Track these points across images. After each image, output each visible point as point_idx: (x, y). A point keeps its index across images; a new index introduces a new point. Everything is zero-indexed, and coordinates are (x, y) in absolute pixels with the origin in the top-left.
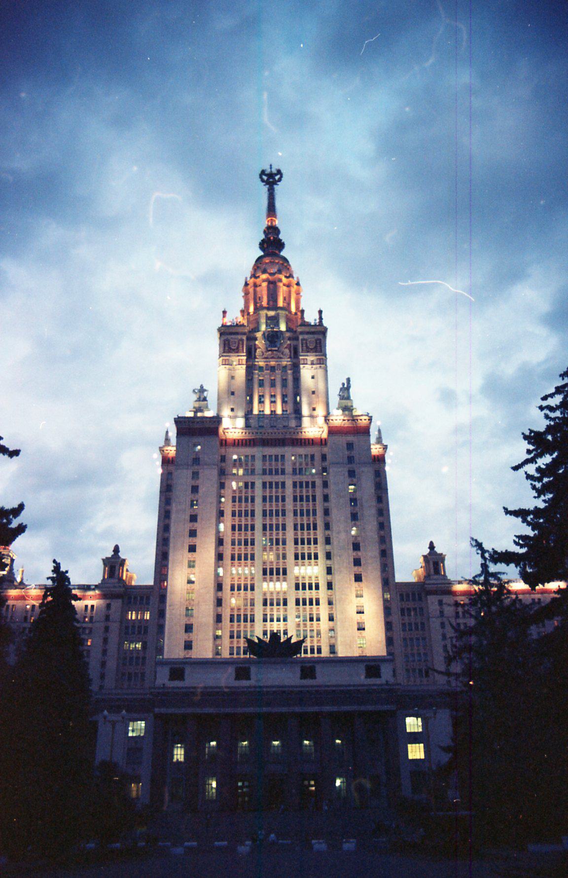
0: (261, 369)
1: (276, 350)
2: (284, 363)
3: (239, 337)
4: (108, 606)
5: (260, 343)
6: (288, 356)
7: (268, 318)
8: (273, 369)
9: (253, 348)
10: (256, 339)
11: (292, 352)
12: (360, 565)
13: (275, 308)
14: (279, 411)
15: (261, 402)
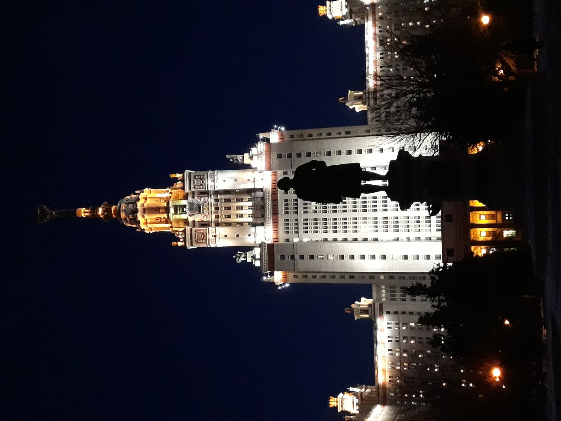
0: (217, 217)
1: (203, 207)
2: (213, 201)
3: (194, 233)
4: (388, 313)
5: (198, 218)
6: (207, 198)
7: (176, 213)
8: (217, 209)
9: (200, 223)
10: (194, 221)
11: (202, 195)
12: (361, 150)
13: (167, 210)
14: (250, 204)
15: (241, 216)
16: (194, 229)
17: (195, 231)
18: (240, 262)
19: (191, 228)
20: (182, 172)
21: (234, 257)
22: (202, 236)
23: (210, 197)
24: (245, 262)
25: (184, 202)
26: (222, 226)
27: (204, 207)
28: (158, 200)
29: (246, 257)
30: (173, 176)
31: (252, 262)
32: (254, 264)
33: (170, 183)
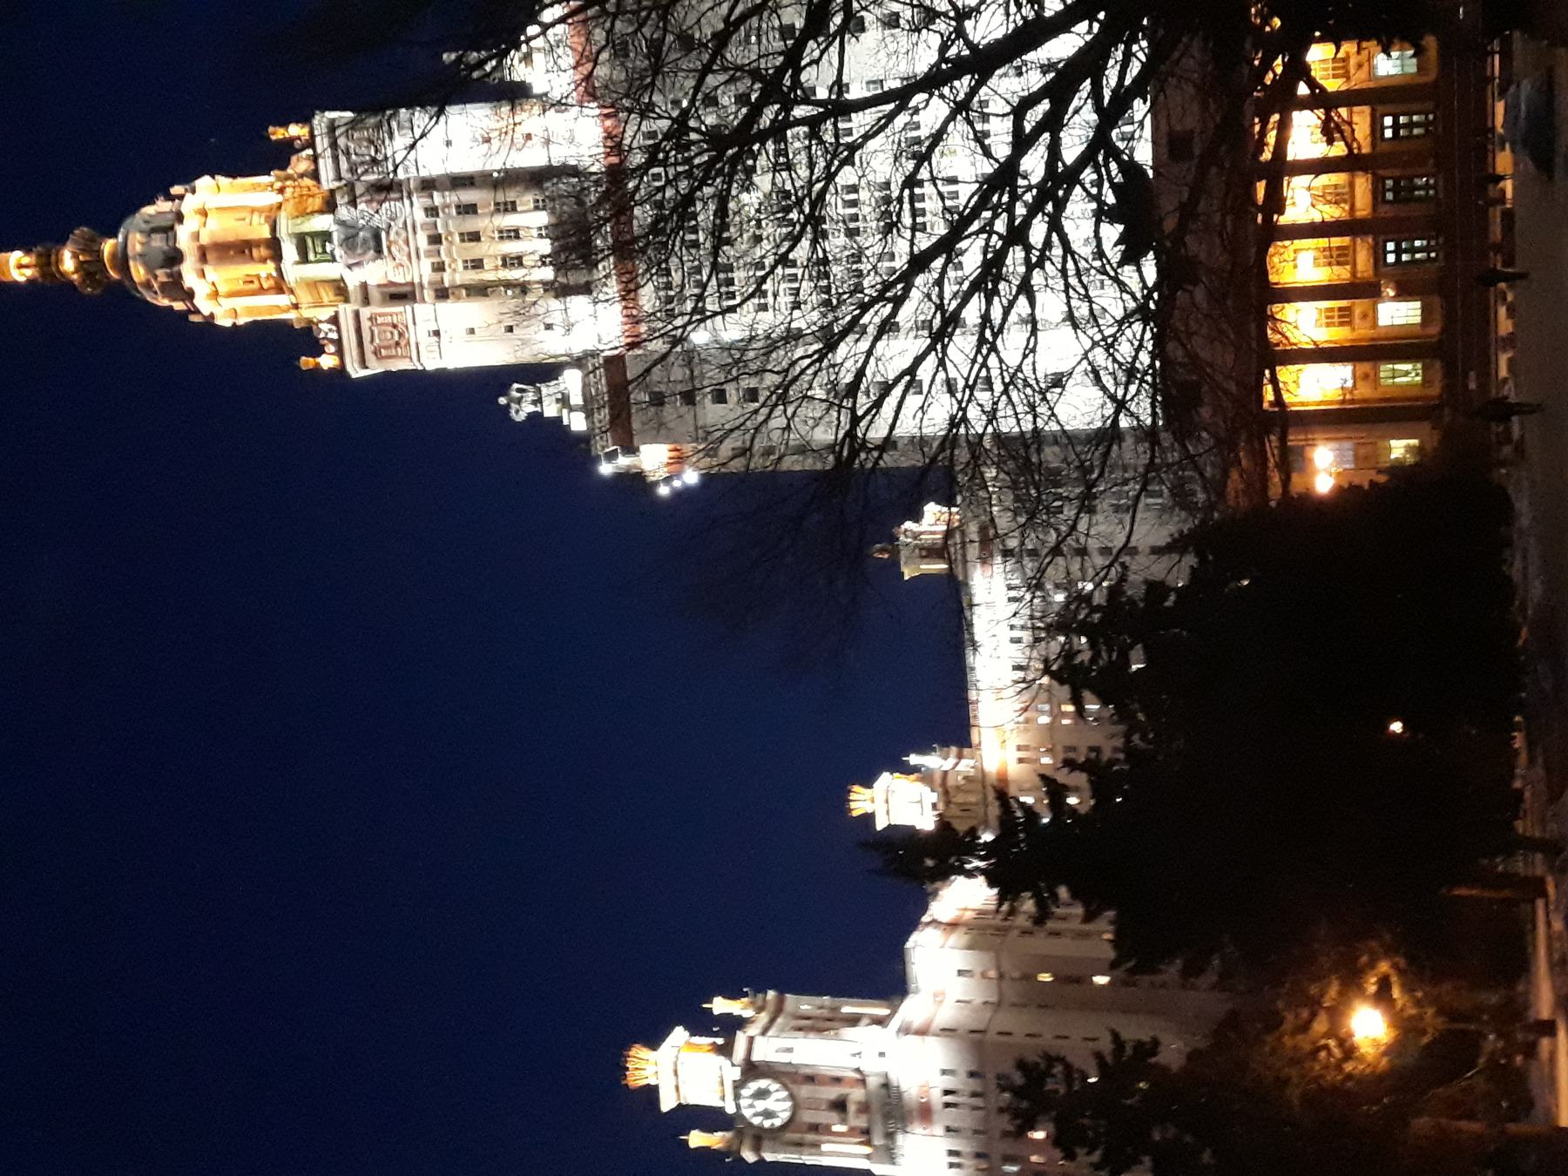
0: (439, 268)
2: (420, 216)
3: (365, 324)
5: (375, 272)
6: (399, 204)
7: (304, 259)
8: (435, 239)
9: (385, 290)
13: (274, 247)
14: (543, 218)
16: (365, 313)
17: (370, 319)
18: (521, 417)
19: (356, 307)
20: (306, 119)
21: (502, 401)
22: (392, 333)
23: (407, 202)
24: (535, 417)
25: (323, 222)
26: (459, 298)
27: (392, 236)
28: (242, 215)
29: (538, 401)
30: (278, 134)
31: (559, 419)
32: (565, 422)
33: (276, 158)
